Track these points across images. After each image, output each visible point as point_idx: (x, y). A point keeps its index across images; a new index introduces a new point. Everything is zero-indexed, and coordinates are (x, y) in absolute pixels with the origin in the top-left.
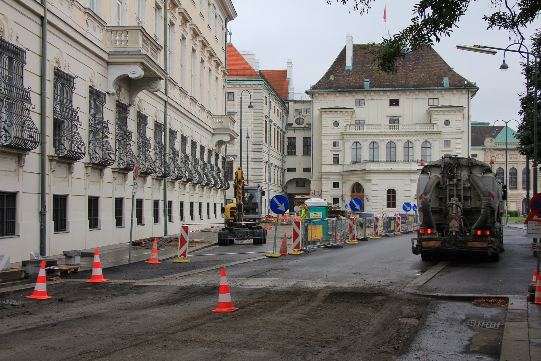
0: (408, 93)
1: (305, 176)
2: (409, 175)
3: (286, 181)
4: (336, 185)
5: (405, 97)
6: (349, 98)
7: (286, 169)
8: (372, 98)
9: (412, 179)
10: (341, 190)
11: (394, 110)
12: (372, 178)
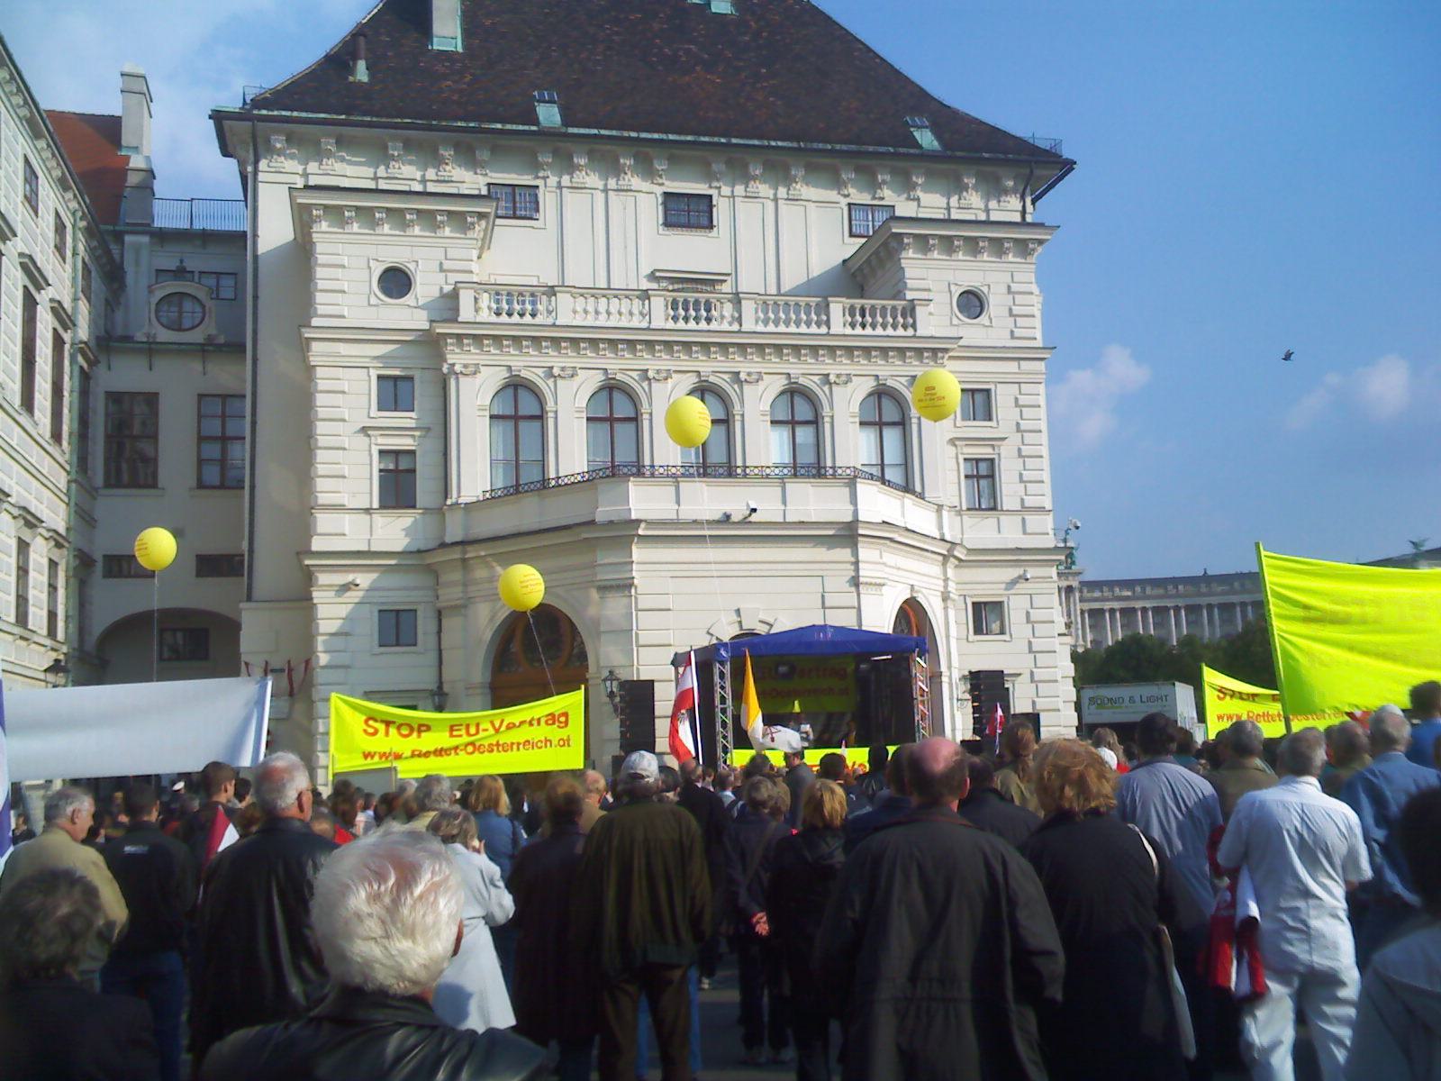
1: (208, 595)
10: (433, 656)
11: (691, 252)
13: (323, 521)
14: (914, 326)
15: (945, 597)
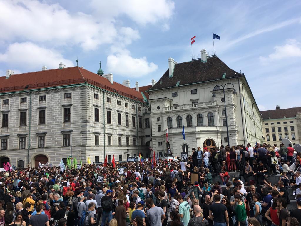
0: (201, 85)
2: (195, 135)
3: (145, 143)
4: (160, 144)
5: (200, 88)
6: (169, 93)
7: (145, 136)
8: (181, 91)
9: (197, 137)
11: (194, 97)
12: (172, 139)
13: (153, 133)
14: (214, 104)
15: (218, 138)
